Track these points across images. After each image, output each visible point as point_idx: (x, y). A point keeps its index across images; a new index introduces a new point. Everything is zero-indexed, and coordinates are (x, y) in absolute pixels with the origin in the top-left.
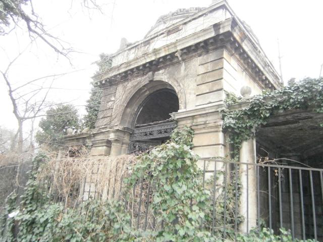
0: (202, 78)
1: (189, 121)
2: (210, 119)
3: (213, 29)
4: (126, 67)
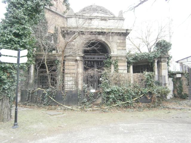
1: (115, 58)
2: (122, 58)
3: (125, 30)
4: (85, 30)
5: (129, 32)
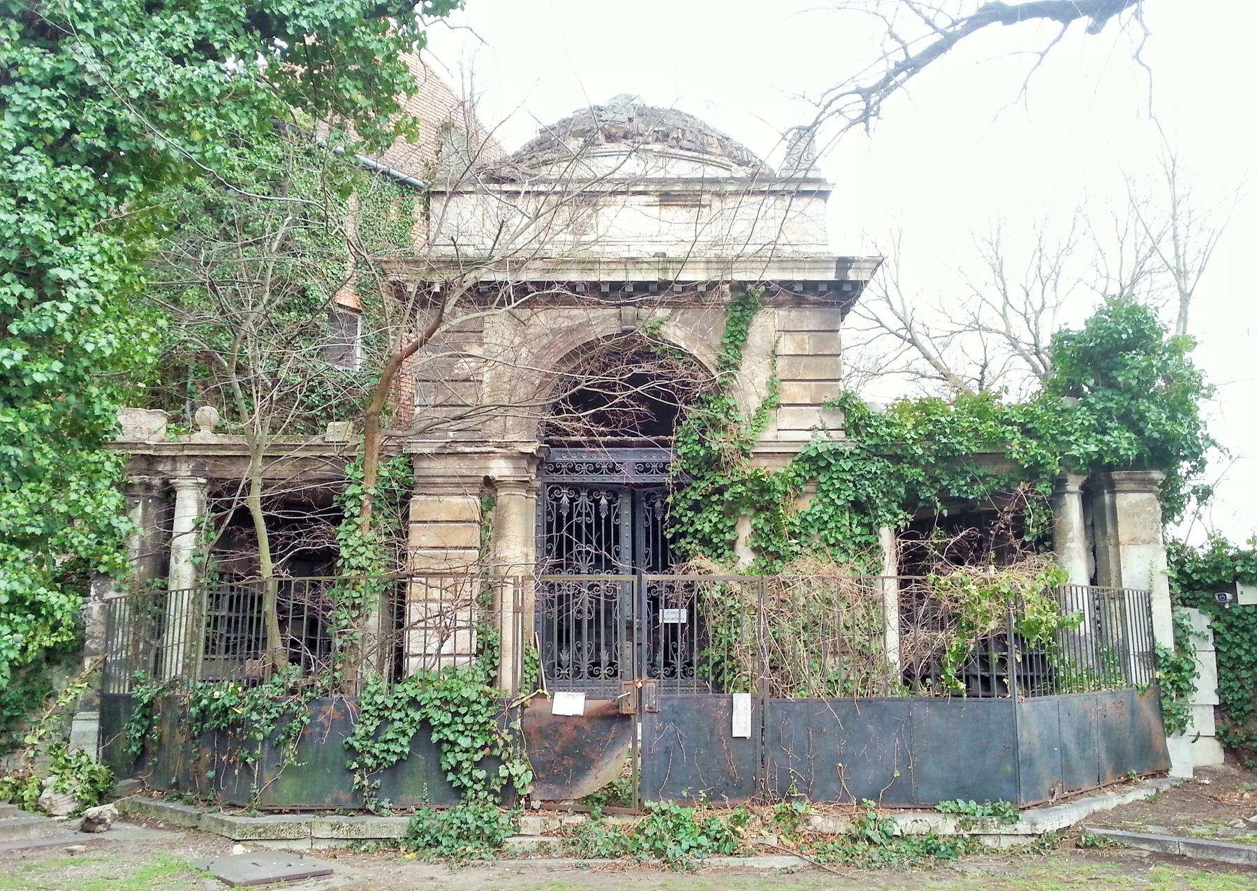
0: (791, 365)
3: (834, 265)
5: (863, 277)
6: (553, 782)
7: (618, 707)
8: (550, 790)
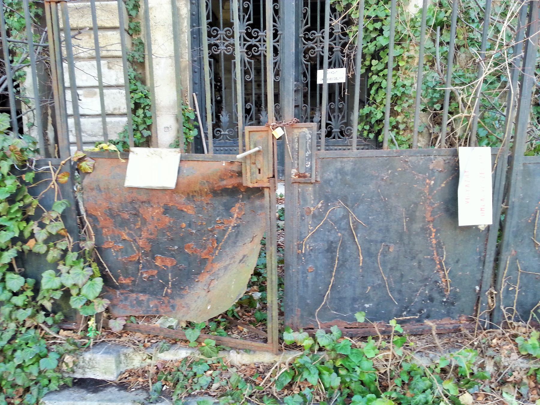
6: (144, 291)
7: (240, 174)
8: (140, 303)
